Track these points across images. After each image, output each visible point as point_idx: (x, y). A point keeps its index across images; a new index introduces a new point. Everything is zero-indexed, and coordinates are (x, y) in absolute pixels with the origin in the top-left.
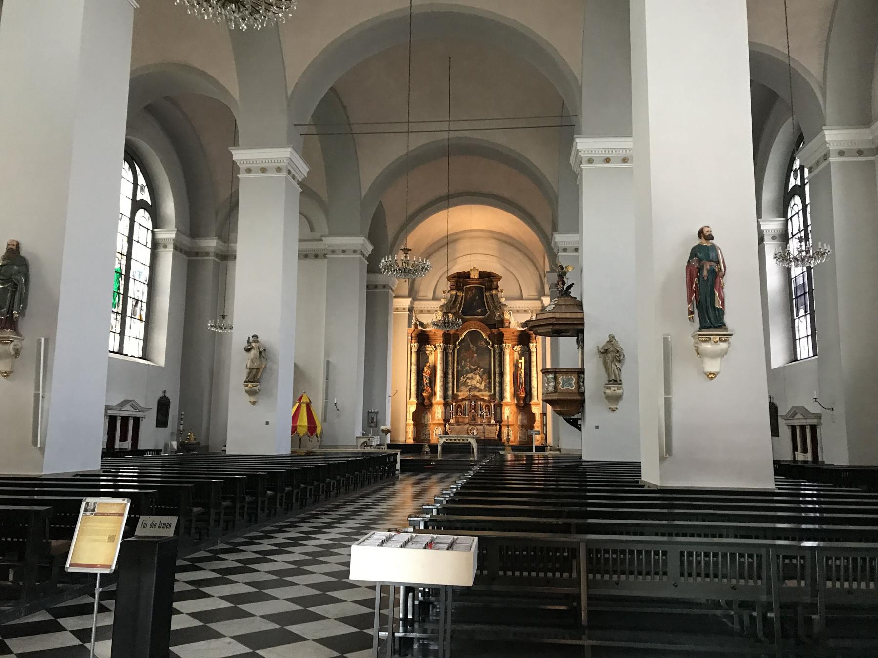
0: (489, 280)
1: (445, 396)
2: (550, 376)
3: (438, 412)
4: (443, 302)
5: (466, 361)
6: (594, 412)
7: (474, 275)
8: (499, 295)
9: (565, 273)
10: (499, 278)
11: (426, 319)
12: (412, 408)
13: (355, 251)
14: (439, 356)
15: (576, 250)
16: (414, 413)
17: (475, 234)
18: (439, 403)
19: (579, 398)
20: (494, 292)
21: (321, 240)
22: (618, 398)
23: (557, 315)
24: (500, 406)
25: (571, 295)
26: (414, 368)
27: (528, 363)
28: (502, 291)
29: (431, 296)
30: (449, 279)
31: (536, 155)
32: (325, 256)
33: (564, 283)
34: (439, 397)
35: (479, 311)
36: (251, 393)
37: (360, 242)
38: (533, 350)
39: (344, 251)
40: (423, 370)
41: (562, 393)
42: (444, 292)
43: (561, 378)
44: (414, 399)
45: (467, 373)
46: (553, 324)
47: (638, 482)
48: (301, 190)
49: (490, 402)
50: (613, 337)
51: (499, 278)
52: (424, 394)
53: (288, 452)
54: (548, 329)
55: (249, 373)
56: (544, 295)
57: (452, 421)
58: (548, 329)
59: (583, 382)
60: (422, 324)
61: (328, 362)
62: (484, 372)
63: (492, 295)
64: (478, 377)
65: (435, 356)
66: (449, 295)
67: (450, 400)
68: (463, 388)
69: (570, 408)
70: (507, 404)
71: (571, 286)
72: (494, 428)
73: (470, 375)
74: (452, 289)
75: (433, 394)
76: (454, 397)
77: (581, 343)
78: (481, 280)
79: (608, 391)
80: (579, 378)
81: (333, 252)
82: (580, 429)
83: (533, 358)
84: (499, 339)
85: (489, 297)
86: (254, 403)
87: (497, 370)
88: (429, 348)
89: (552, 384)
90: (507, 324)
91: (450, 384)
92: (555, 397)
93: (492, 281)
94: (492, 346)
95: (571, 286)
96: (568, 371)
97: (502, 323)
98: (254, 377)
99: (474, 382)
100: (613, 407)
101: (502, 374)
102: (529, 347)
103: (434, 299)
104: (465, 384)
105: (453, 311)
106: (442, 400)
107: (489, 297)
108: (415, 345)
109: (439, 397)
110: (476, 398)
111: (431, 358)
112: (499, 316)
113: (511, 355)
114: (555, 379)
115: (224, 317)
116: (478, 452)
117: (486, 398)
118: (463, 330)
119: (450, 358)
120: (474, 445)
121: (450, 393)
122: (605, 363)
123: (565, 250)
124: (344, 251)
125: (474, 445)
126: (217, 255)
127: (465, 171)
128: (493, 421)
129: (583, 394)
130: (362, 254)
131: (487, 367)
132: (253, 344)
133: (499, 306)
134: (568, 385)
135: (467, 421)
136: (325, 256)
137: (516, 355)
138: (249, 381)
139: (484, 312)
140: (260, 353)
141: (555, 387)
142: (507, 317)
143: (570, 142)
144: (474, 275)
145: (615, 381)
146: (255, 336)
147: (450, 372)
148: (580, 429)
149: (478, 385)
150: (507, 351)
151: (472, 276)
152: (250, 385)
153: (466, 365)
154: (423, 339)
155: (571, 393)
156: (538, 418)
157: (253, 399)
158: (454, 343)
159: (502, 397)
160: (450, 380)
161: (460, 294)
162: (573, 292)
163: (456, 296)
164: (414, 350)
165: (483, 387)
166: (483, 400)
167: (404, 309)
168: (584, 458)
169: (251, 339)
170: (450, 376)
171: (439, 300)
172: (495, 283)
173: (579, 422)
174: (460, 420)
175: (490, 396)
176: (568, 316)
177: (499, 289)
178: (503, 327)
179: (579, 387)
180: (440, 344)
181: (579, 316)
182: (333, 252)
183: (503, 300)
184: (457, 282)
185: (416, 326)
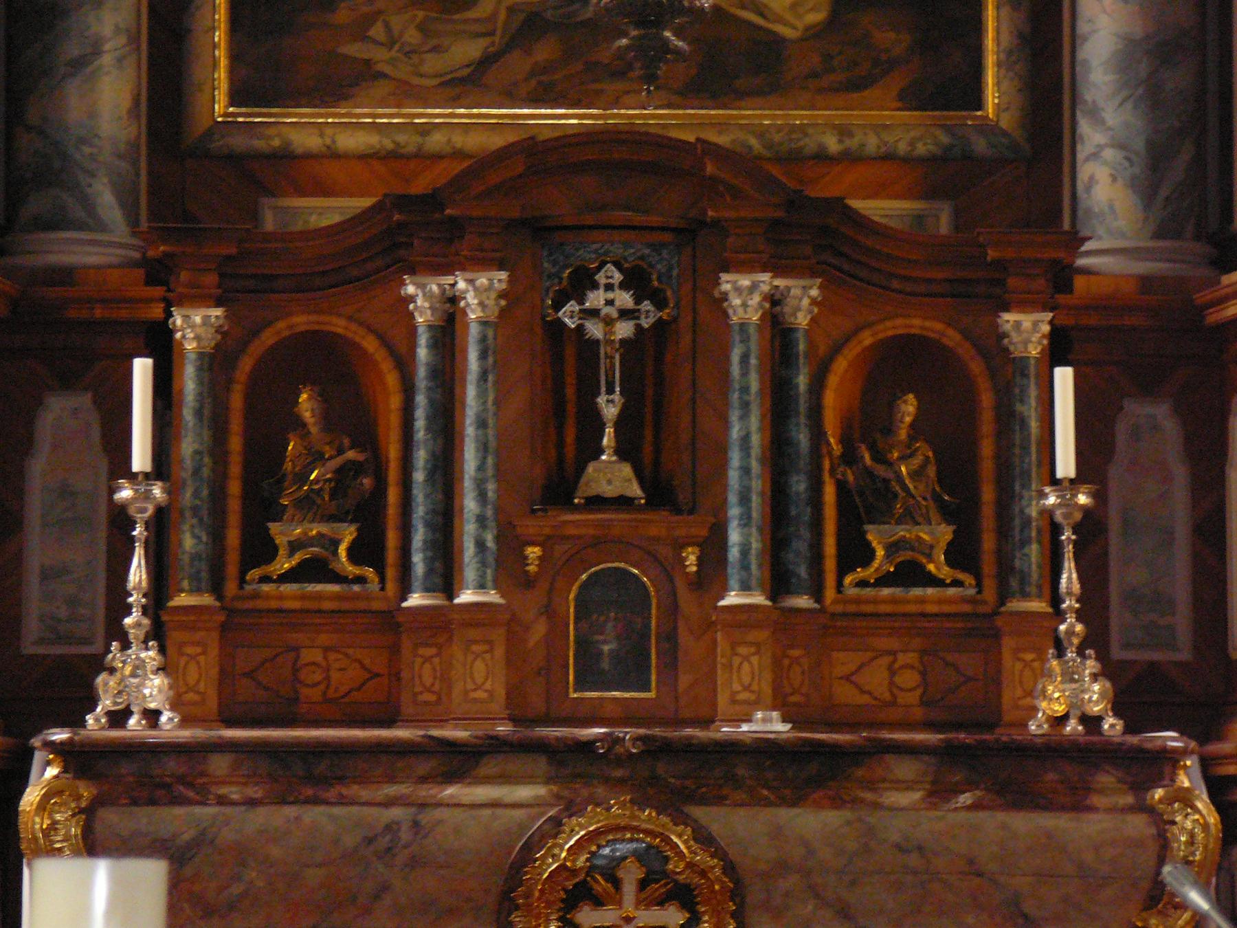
72: (1100, 826)
76: (199, 194)
110: (686, 213)
128: (1068, 694)
135: (472, 690)
174: (328, 664)
175: (945, 175)
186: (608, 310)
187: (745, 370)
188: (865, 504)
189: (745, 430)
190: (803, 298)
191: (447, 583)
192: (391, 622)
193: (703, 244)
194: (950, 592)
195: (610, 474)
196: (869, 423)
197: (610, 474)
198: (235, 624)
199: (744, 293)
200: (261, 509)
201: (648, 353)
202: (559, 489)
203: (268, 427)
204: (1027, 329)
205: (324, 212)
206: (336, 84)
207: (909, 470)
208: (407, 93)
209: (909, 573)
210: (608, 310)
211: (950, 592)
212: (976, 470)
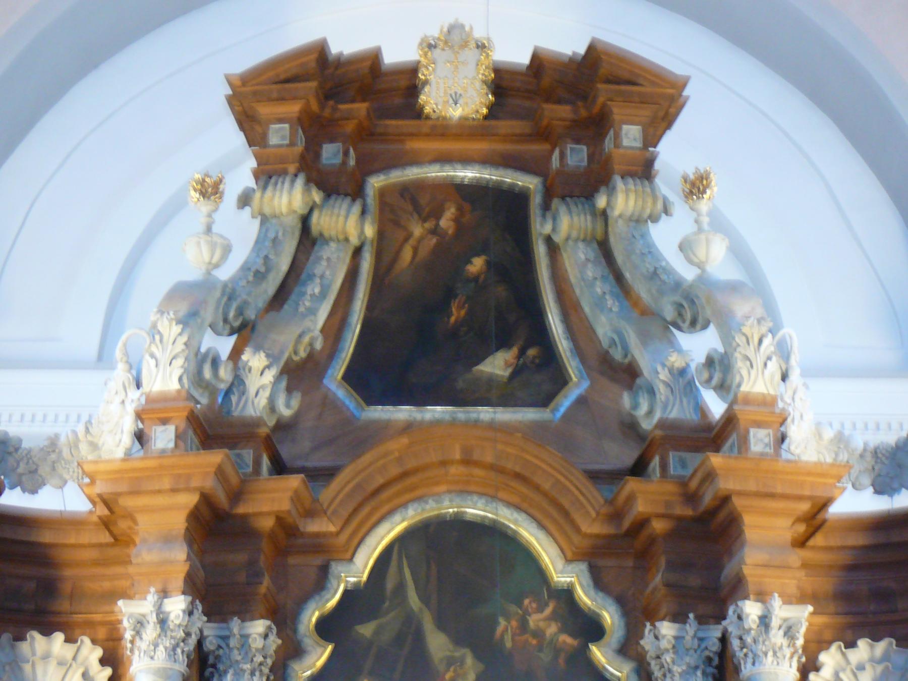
0: (580, 113)
7: (455, 95)
8: (665, 236)
10: (661, 99)
20: (623, 200)
28: (696, 187)
30: (250, 100)
35: (497, 365)
42: (210, 190)
51: (661, 99)
66: (241, 232)
78: (505, 126)
85: (580, 263)
90: (759, 440)
93: (595, 127)
94: (628, 648)
107: (580, 263)
118: (371, 503)
144: (455, 95)
151: (432, 100)
158: (284, 619)
161: (347, 225)
163: (308, 239)
172: (631, 135)
184: (315, 128)
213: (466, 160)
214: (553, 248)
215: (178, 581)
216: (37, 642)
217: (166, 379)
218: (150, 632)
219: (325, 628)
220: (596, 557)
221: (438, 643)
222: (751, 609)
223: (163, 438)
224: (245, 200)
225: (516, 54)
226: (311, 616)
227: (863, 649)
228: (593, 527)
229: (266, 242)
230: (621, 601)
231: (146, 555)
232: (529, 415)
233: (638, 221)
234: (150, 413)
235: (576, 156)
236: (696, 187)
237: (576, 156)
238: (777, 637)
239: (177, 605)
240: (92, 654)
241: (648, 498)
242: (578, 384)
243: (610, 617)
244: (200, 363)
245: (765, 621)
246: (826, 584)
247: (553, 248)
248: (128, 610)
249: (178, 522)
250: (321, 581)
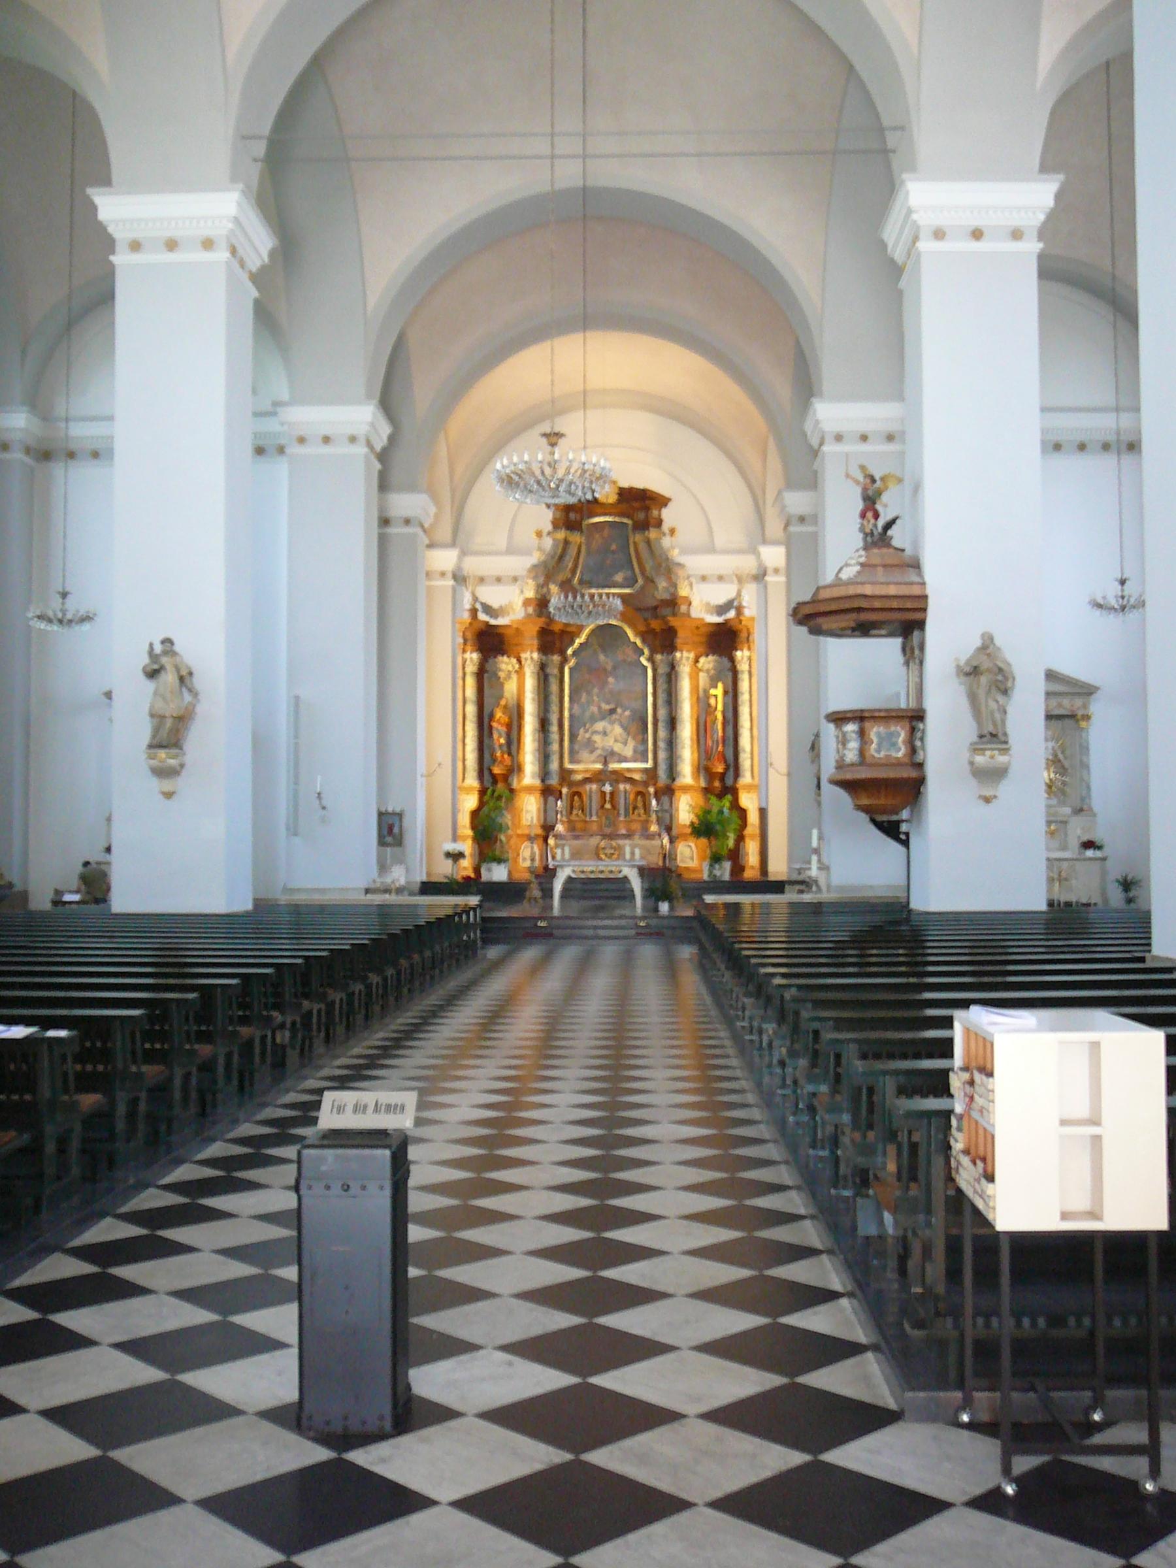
0: (641, 505)
1: (544, 774)
2: (851, 727)
3: (530, 808)
4: (535, 558)
5: (589, 693)
6: (946, 807)
7: (606, 494)
8: (666, 542)
9: (879, 493)
10: (663, 502)
11: (492, 596)
12: (470, 802)
13: (353, 439)
14: (530, 683)
15: (890, 438)
16: (475, 814)
17: (616, 404)
18: (529, 790)
19: (913, 774)
20: (653, 534)
21: (274, 414)
22: (996, 774)
23: (868, 590)
24: (668, 792)
25: (896, 543)
26: (471, 709)
27: (733, 694)
28: (672, 531)
29: (502, 544)
31: (771, 219)
32: (281, 450)
33: (877, 516)
34: (530, 774)
35: (619, 577)
36: (162, 772)
37: (362, 417)
38: (743, 667)
39: (326, 440)
40: (492, 716)
41: (876, 765)
42: (539, 534)
43: (875, 732)
44: (472, 781)
45: (593, 720)
46: (859, 610)
47: (1142, 960)
48: (255, 293)
49: (646, 784)
50: (991, 639)
51: (663, 502)
52: (497, 770)
53: (249, 906)
54: (849, 620)
55: (156, 730)
56: (765, 542)
57: (560, 828)
58: (849, 620)
59: (922, 739)
60: (487, 609)
61: (297, 698)
62: (632, 718)
63: (648, 542)
64: (618, 730)
65: (520, 678)
66: (548, 543)
67: (554, 781)
68: (584, 755)
69: (889, 799)
70: (686, 789)
71: (889, 525)
72: (657, 842)
73: (600, 726)
74: (556, 525)
75: (516, 768)
76: (565, 775)
77: (913, 654)
79: (980, 759)
80: (913, 730)
81: (302, 440)
82: (906, 843)
83: (744, 685)
84: (664, 640)
85: (642, 546)
86: (169, 795)
87: (662, 713)
88: (506, 664)
89: (854, 745)
90: (683, 608)
91: (555, 747)
92: (863, 774)
93: (647, 509)
94: (651, 659)
95: (889, 525)
96: (888, 716)
97: (673, 602)
98: (169, 735)
99: (609, 742)
100: (988, 793)
101: (673, 723)
102: (732, 660)
103: (511, 550)
104: (590, 745)
105: (561, 577)
106: (537, 782)
107: (642, 546)
108: (473, 657)
109: (530, 774)
111: (510, 688)
112: (666, 589)
113: (694, 677)
114: (862, 733)
115: (64, 595)
116: (645, 897)
117: (637, 777)
119: (554, 688)
120: (636, 885)
121: (554, 766)
122: (973, 698)
123: (839, 438)
124: (326, 440)
125: (636, 885)
126: (28, 450)
127: (606, 252)
128: (654, 828)
129: (920, 766)
130: (369, 444)
131: (640, 702)
132: (164, 660)
133: (667, 568)
134: (887, 746)
135: (595, 827)
136: (281, 450)
137: (703, 678)
138: (161, 746)
139: (630, 582)
140: (182, 679)
141: (862, 752)
142: (683, 592)
143: (889, 188)
145: (993, 735)
146: (167, 642)
147: (554, 718)
148: (906, 843)
149: (617, 748)
150: (685, 670)
152: (162, 754)
153: (590, 702)
154: (490, 642)
155: (898, 764)
156: (753, 818)
157: (167, 785)
158: (562, 652)
159: (672, 773)
160: (554, 736)
161: (576, 538)
162: (897, 536)
163: (566, 542)
164: (471, 668)
165: (628, 751)
166: (631, 780)
167: (443, 574)
168: (913, 906)
169: (158, 649)
170: (554, 728)
171: (528, 553)
172: (655, 513)
173: (904, 827)
174: (579, 825)
175: (646, 770)
176: (892, 590)
177: (666, 527)
178: (674, 615)
179: (913, 751)
180: (531, 657)
181: (916, 591)
182: (302, 440)
183: (676, 555)
185: (474, 612)
186: (608, 788)
187: (622, 795)
188: (635, 808)
189: (622, 801)
190: (628, 787)
191: (591, 816)
192: (586, 822)
193: (617, 782)
194: (644, 817)
195: (608, 806)
196: (636, 799)
197: (608, 806)
198: (570, 821)
199: (621, 787)
200: (572, 808)
201: (612, 794)
202: (602, 807)
203: (572, 801)
204: (652, 790)
205: (579, 777)
206: (578, 762)
207: (640, 804)
208: (586, 763)
209: (639, 815)
210: (608, 788)
211: (644, 817)
212: (647, 807)
213: (610, 514)
214: (635, 543)
215: (536, 647)
216: (500, 658)
217: (530, 593)
218: (529, 662)
219: (575, 653)
220: (643, 636)
221: (602, 657)
222: (678, 655)
223: (530, 610)
224: (549, 534)
225: (625, 484)
226: (570, 652)
227: (711, 658)
228: (642, 628)
229: (555, 545)
230: (649, 646)
231: (527, 642)
232: (627, 591)
233: (658, 539)
234: (526, 602)
235: (641, 516)
236: (672, 531)
237: (641, 516)
238: (684, 661)
239: (535, 655)
240: (514, 661)
241: (656, 625)
242: (640, 581)
243: (646, 651)
244: (539, 587)
245: (681, 658)
246: (704, 639)
247: (635, 543)
248: (523, 656)
249: (535, 633)
250: (572, 642)
